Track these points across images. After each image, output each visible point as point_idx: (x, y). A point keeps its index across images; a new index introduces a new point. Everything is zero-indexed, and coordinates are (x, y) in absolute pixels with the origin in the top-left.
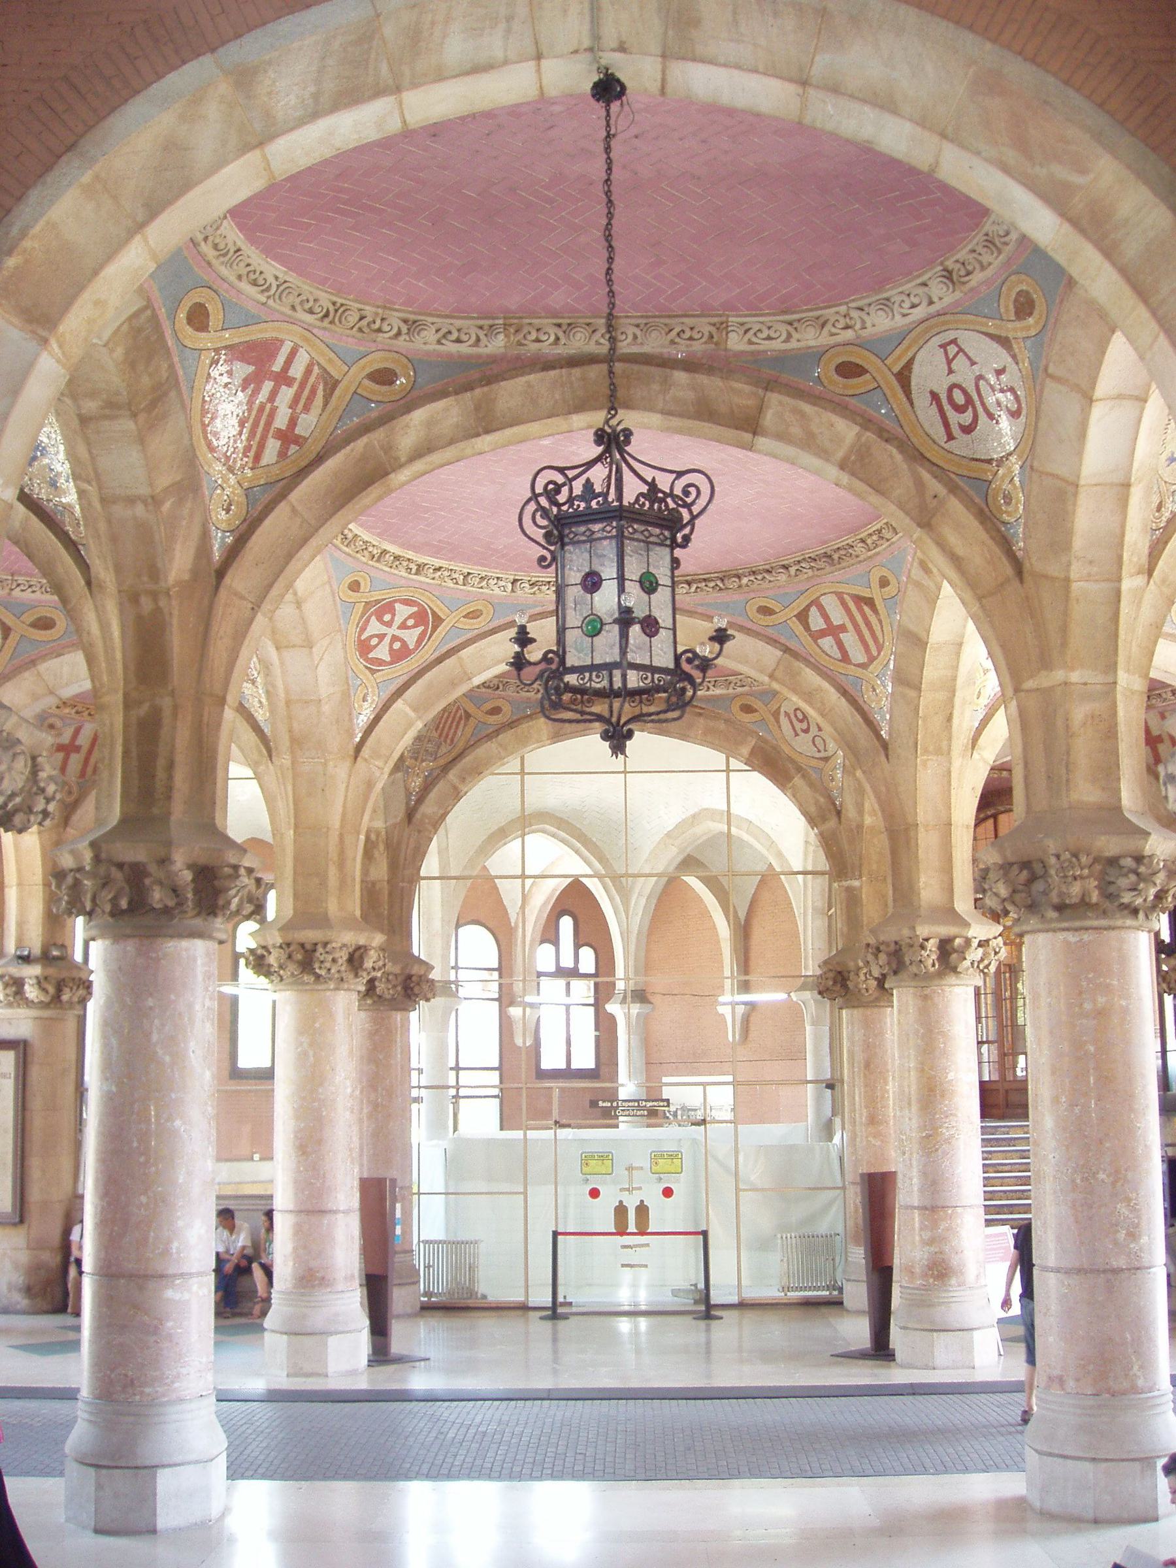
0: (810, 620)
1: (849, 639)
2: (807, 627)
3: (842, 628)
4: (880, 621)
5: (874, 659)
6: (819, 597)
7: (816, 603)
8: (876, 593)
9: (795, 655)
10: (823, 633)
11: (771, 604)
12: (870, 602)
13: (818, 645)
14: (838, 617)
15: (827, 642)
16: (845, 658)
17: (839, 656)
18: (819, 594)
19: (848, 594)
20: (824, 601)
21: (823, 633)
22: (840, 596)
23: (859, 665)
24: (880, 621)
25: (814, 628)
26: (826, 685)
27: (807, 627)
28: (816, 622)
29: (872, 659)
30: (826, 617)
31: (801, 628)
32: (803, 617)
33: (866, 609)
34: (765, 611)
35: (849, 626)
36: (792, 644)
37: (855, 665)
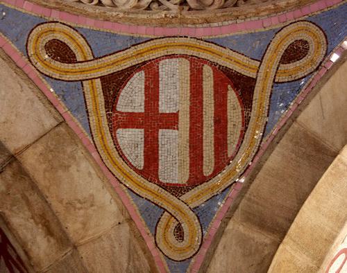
0: (123, 93)
1: (173, 143)
2: (111, 103)
3: (171, 121)
4: (246, 122)
5: (204, 180)
6: (158, 60)
7: (150, 69)
8: (265, 75)
9: (73, 136)
10: (131, 121)
11: (77, 45)
12: (245, 87)
13: (114, 138)
14: (174, 98)
15: (131, 138)
16: (150, 168)
17: (140, 163)
18: (162, 53)
19: (212, 64)
20: (165, 68)
21: (131, 121)
22: (196, 66)
23: (166, 187)
24: (246, 122)
25: (123, 106)
26: (105, 198)
27: (111, 103)
28: (132, 98)
29: (197, 178)
30: (152, 94)
31: (101, 99)
32: (113, 84)
33: (232, 96)
34: (60, 52)
35: (184, 121)
36: (75, 122)
37: (161, 185)
